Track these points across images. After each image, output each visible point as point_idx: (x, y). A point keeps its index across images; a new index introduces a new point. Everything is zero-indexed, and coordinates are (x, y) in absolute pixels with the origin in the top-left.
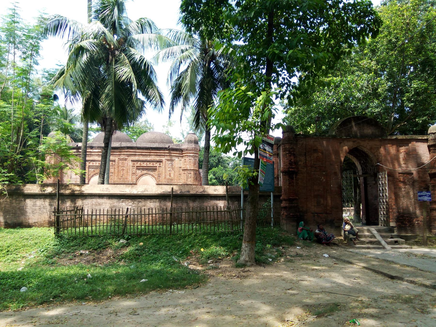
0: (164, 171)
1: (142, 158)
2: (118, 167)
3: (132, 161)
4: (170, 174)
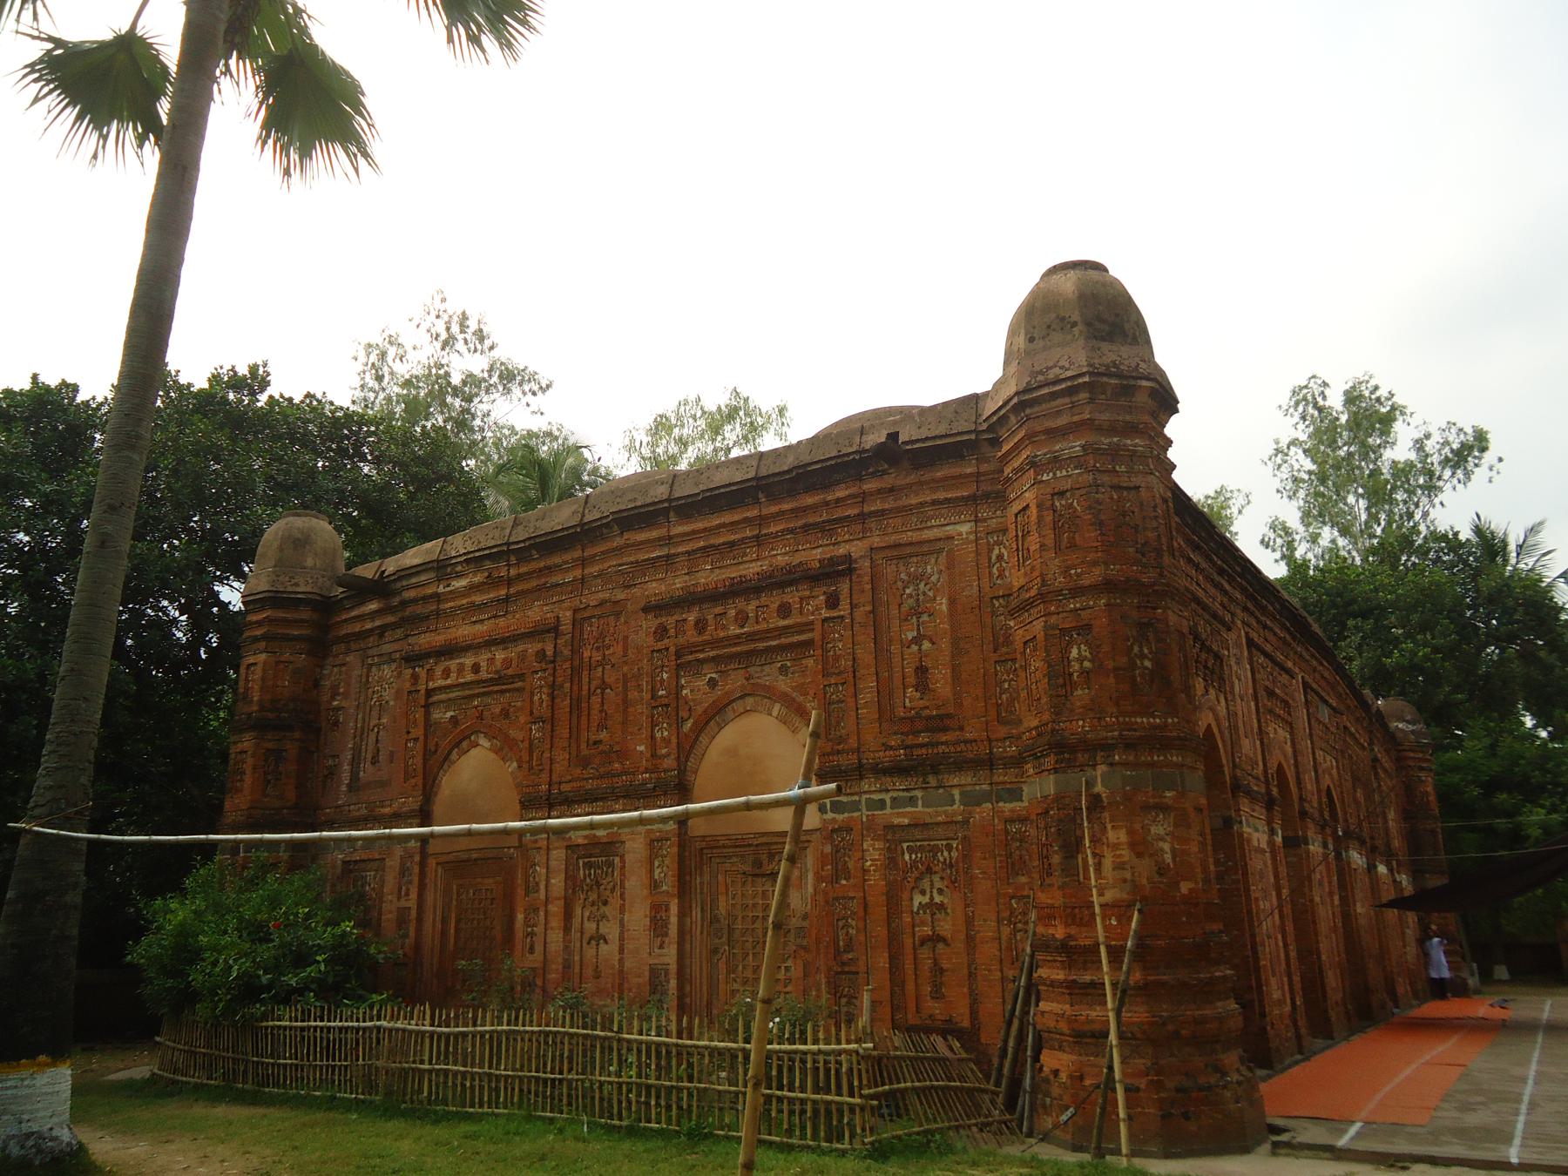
0: (865, 654)
1: (708, 576)
2: (576, 673)
3: (655, 608)
4: (921, 671)
